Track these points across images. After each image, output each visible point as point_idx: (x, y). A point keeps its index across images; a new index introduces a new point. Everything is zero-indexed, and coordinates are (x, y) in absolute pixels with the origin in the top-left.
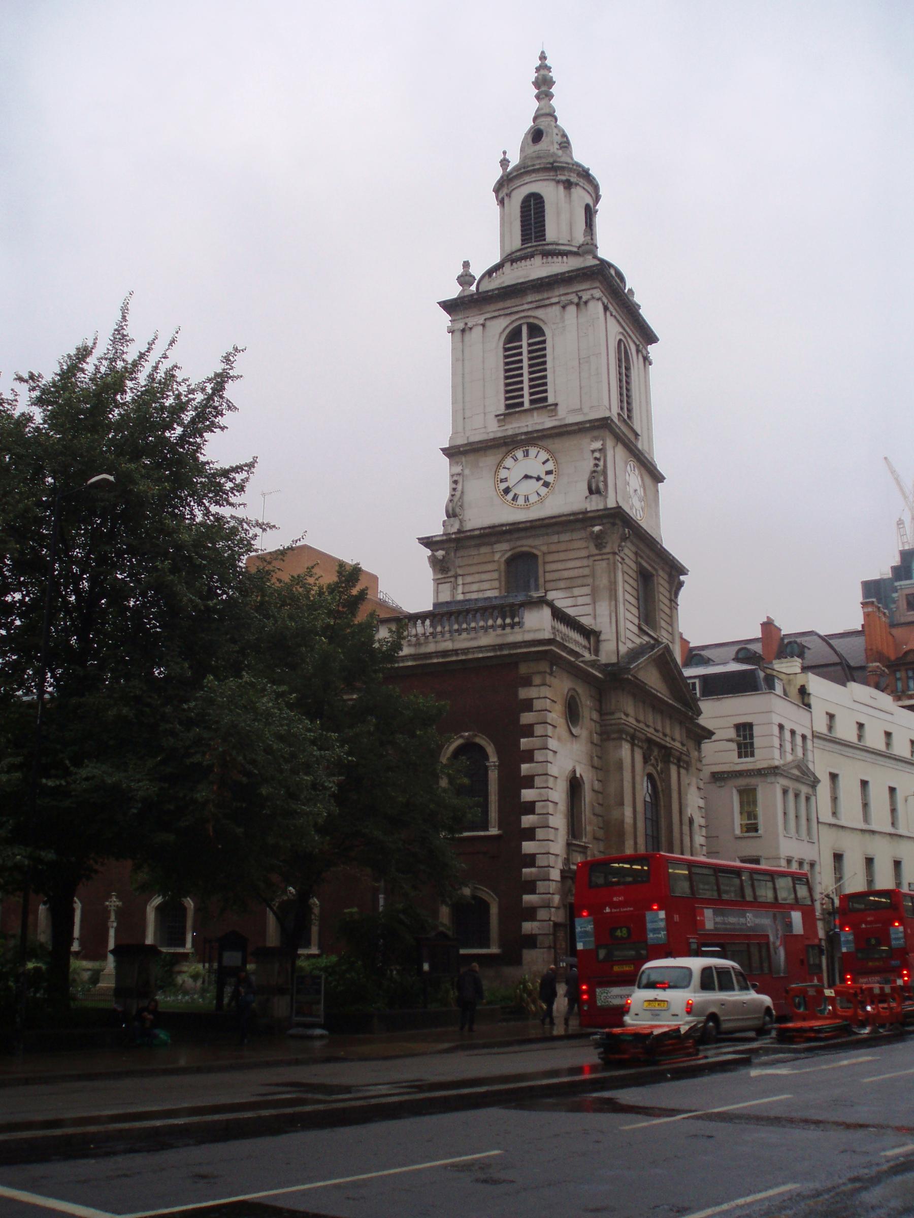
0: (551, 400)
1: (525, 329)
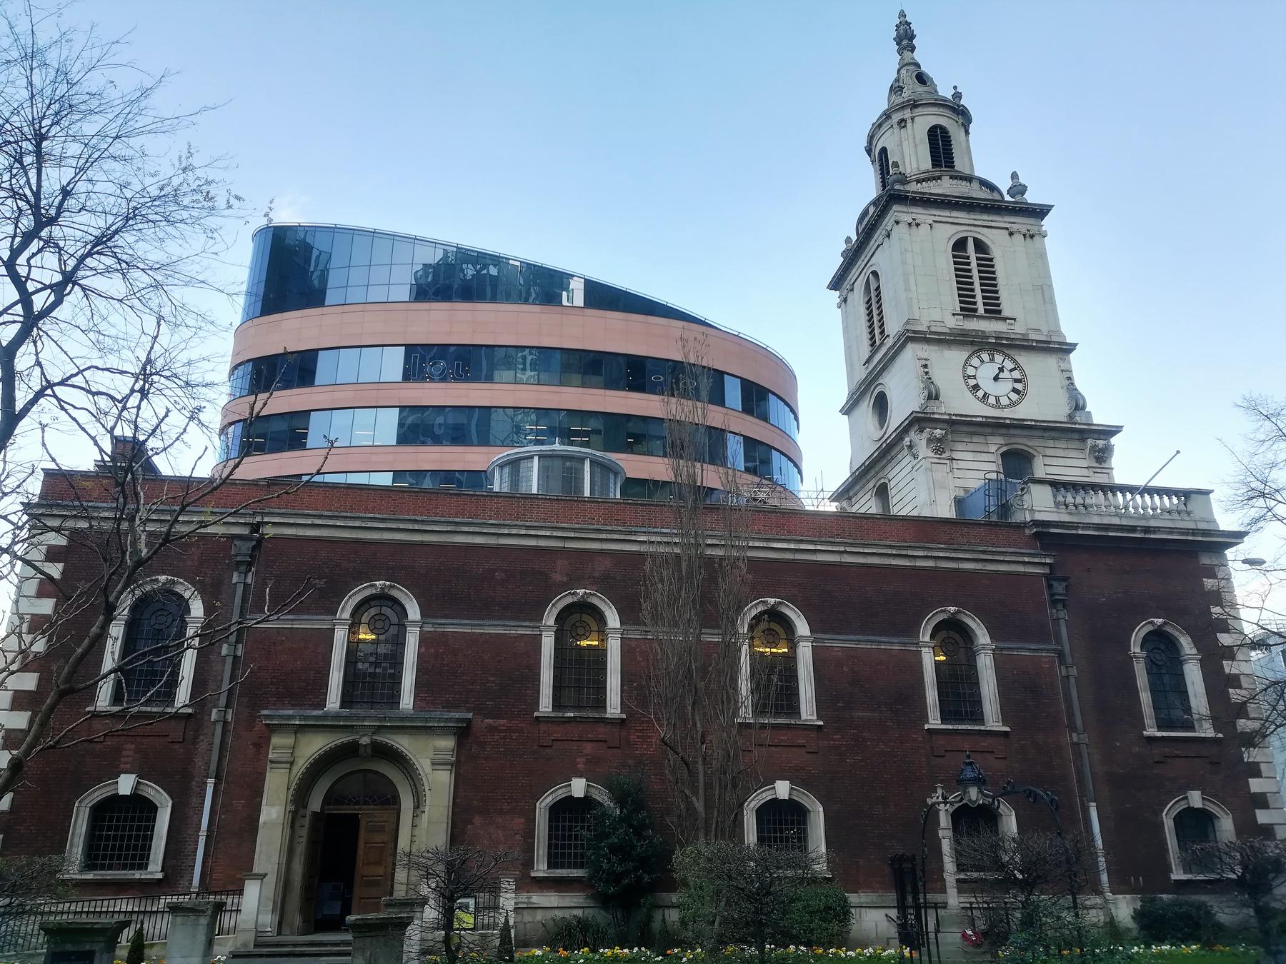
0: (1005, 313)
1: (970, 242)
